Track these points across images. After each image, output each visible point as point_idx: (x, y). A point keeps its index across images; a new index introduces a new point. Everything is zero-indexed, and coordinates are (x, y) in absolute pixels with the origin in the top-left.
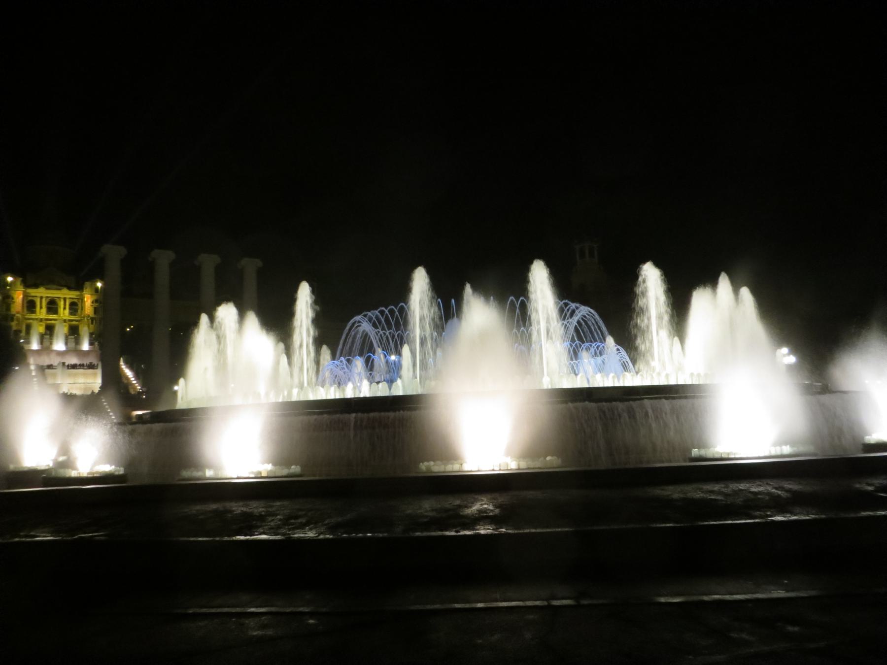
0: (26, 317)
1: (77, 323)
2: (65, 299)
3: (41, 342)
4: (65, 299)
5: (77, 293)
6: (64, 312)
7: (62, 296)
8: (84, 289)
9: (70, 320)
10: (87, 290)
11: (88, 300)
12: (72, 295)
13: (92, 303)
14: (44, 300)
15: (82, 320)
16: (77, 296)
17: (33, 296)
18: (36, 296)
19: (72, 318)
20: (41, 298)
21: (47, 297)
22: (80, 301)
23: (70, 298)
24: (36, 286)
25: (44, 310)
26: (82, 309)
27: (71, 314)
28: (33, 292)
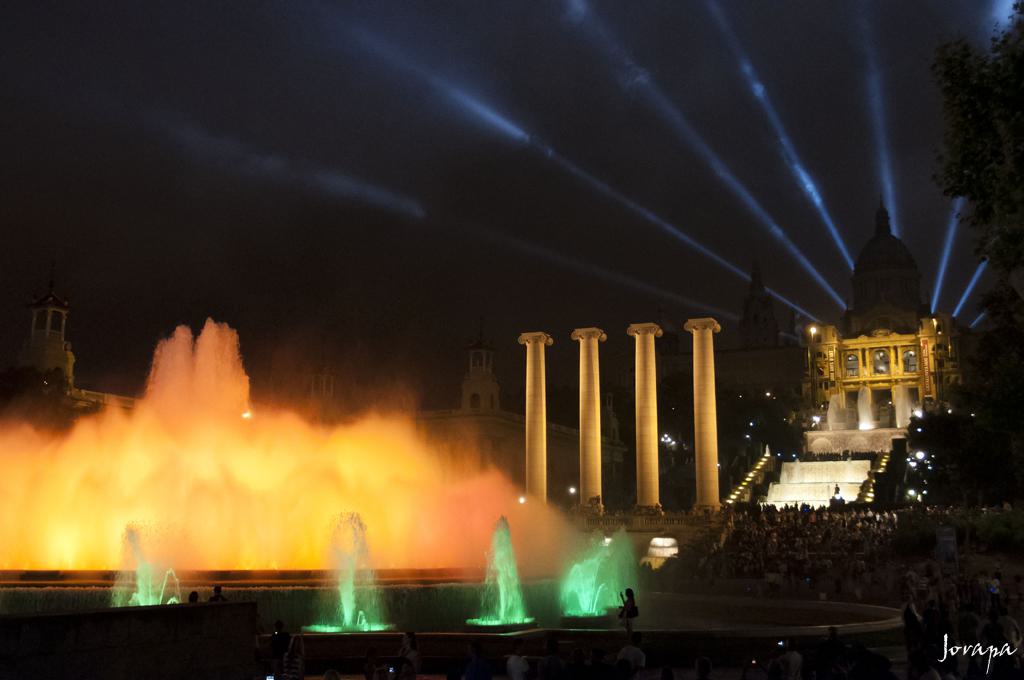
2: (895, 348)
3: (877, 418)
4: (895, 348)
5: (912, 337)
6: (897, 370)
7: (891, 345)
9: (903, 380)
10: (924, 331)
11: (928, 349)
12: (906, 340)
13: (933, 349)
14: (867, 353)
17: (852, 350)
18: (856, 349)
19: (907, 375)
20: (864, 351)
24: (856, 336)
27: (906, 370)
28: (851, 343)
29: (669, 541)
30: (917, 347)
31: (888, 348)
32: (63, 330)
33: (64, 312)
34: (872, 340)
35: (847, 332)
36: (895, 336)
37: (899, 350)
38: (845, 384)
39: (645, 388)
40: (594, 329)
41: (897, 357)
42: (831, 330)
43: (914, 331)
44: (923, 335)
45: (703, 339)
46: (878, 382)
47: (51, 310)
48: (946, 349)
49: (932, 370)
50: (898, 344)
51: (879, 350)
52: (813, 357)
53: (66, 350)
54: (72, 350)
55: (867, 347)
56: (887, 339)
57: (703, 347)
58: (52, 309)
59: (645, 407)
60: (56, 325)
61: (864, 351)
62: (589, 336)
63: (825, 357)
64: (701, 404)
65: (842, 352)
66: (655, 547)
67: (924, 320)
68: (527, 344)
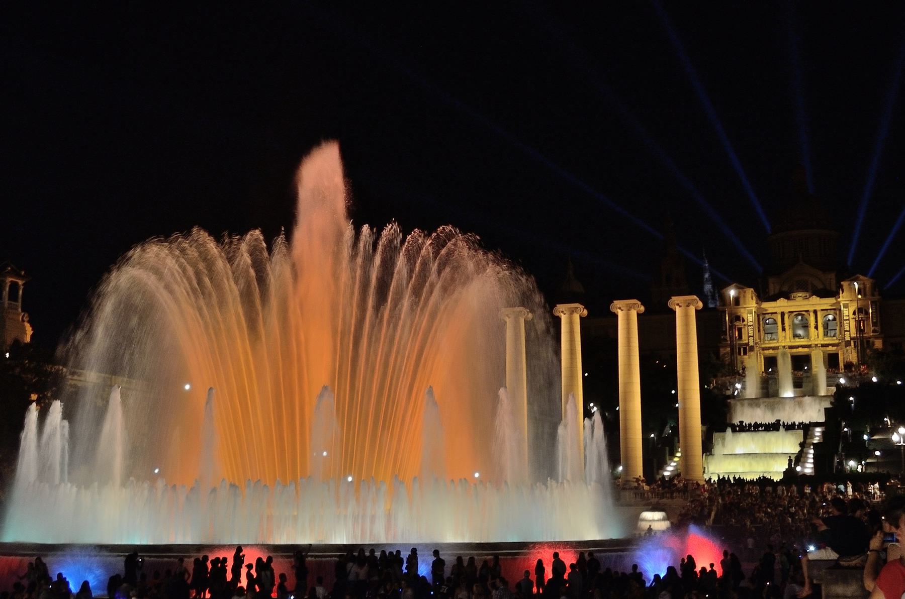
0: (763, 346)
1: (835, 348)
4: (815, 312)
5: (832, 300)
6: (817, 336)
7: (811, 309)
8: (841, 292)
9: (823, 346)
11: (848, 313)
12: (827, 302)
13: (854, 314)
14: (786, 316)
15: (840, 343)
16: (831, 306)
17: (772, 313)
18: (776, 313)
19: (827, 341)
20: (783, 314)
21: (791, 312)
22: (838, 312)
23: (822, 310)
24: (774, 299)
25: (789, 332)
26: (841, 326)
27: (826, 334)
28: (769, 306)
29: (658, 515)
30: (837, 310)
31: (807, 311)
32: (20, 300)
33: (20, 282)
34: (791, 303)
35: (764, 296)
36: (815, 299)
37: (819, 314)
38: (764, 349)
39: (629, 365)
40: (577, 305)
41: (816, 322)
42: (750, 292)
43: (834, 294)
44: (844, 298)
45: (686, 316)
46: (797, 347)
47: (9, 279)
48: (867, 313)
49: (853, 335)
50: (818, 308)
51: (799, 313)
52: (731, 321)
53: (23, 321)
54: (29, 322)
55: (786, 310)
56: (806, 302)
57: (686, 325)
58: (10, 279)
59: (628, 383)
60: (13, 296)
61: (783, 314)
62: (572, 312)
63: (744, 321)
64: (685, 381)
65: (761, 315)
66: (644, 520)
67: (845, 284)
68: (507, 320)
